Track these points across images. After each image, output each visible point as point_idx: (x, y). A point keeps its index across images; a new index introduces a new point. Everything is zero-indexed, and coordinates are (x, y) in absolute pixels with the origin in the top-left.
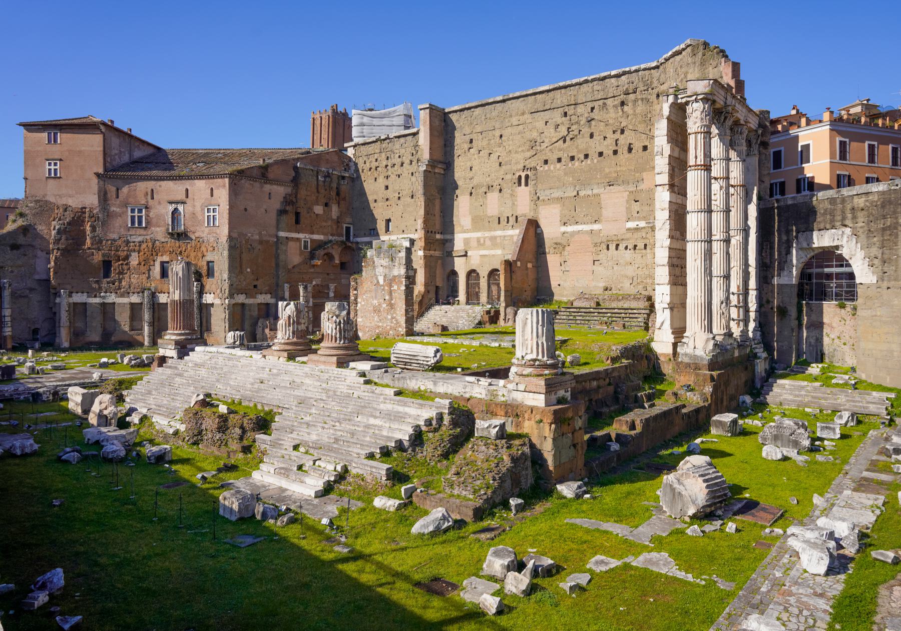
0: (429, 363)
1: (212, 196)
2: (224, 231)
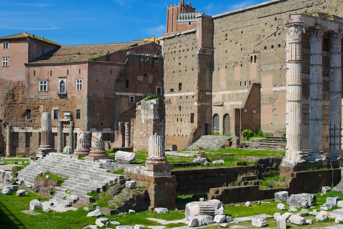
0: (128, 160)
1: (80, 73)
2: (86, 93)
